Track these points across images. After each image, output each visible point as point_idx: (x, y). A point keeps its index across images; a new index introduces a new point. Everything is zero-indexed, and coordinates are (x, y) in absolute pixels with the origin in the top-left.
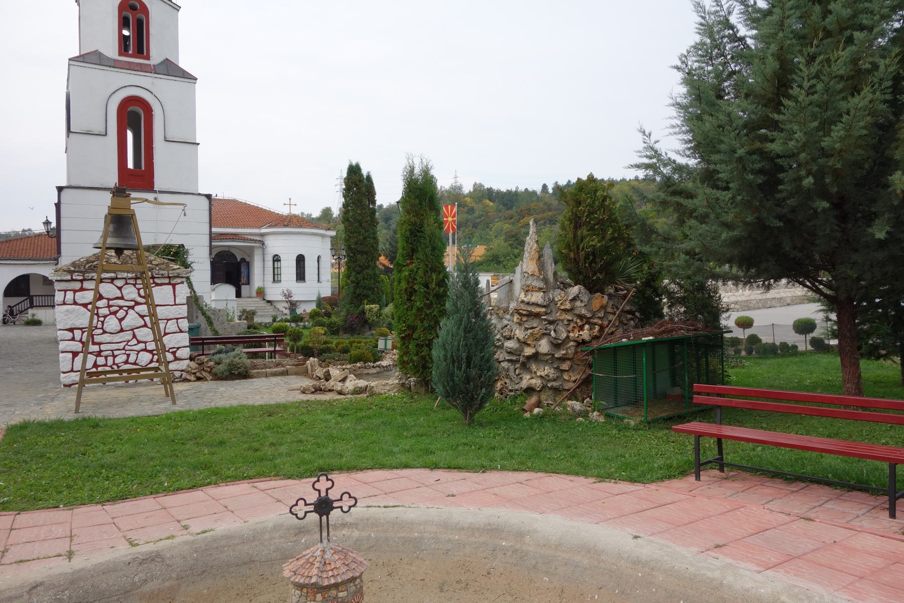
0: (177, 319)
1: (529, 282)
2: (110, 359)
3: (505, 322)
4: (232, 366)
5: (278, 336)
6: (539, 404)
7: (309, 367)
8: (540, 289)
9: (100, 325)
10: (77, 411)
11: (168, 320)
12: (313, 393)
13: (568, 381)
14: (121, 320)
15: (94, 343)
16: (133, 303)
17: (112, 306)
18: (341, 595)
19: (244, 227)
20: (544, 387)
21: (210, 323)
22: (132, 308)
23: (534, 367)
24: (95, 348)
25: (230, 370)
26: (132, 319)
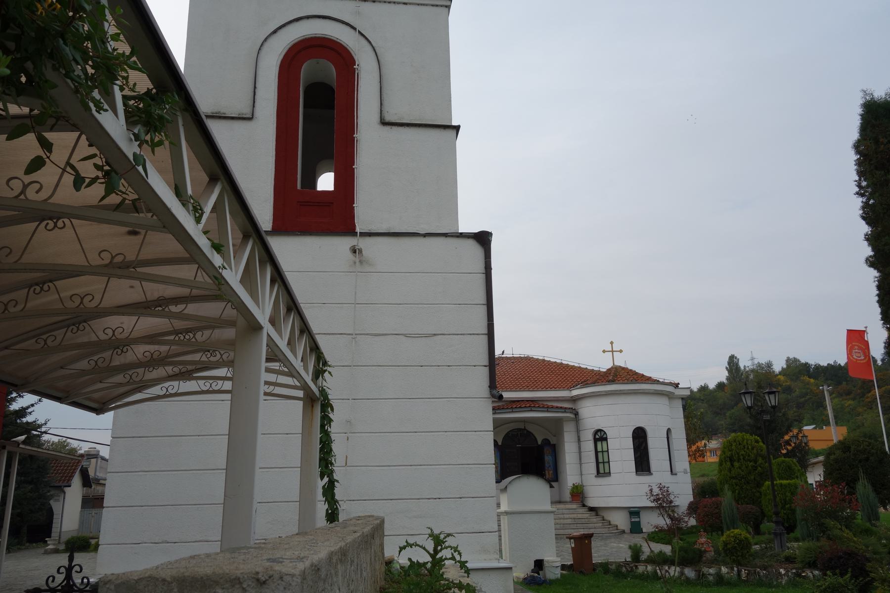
19: (545, 388)
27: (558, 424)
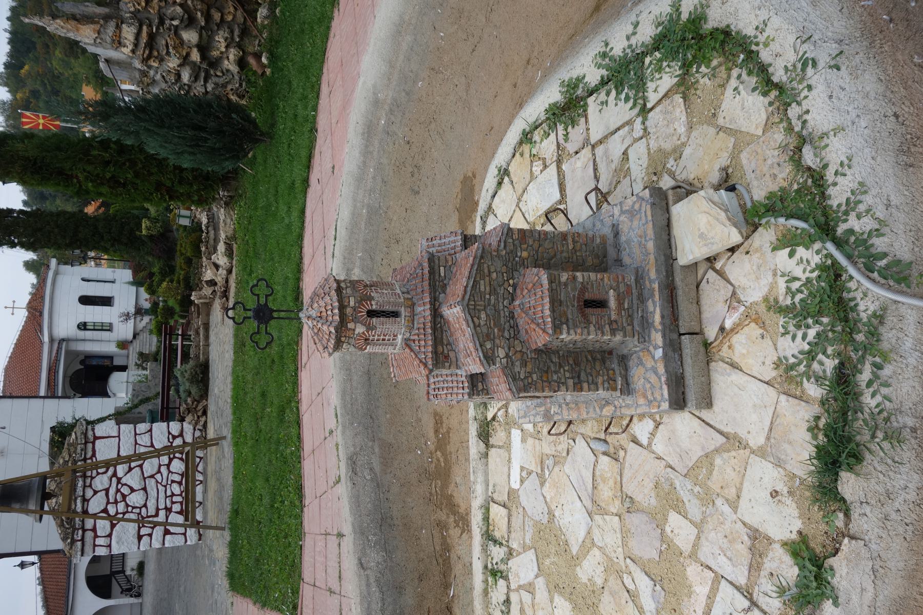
0: (136, 434)
1: (108, 40)
2: (175, 499)
3: (158, 77)
4: (193, 380)
5: (164, 330)
6: (258, 56)
7: (201, 301)
8: (118, 27)
9: (138, 511)
10: (223, 529)
11: (136, 443)
12: (227, 300)
13: (234, 16)
14: (133, 490)
15: (157, 515)
16: (114, 479)
17: (116, 499)
18: (352, 303)
20: (240, 46)
21: (147, 400)
22: (119, 480)
23: (215, 53)
24: (162, 513)
25: (198, 382)
26: (133, 479)
27: (72, 355)
